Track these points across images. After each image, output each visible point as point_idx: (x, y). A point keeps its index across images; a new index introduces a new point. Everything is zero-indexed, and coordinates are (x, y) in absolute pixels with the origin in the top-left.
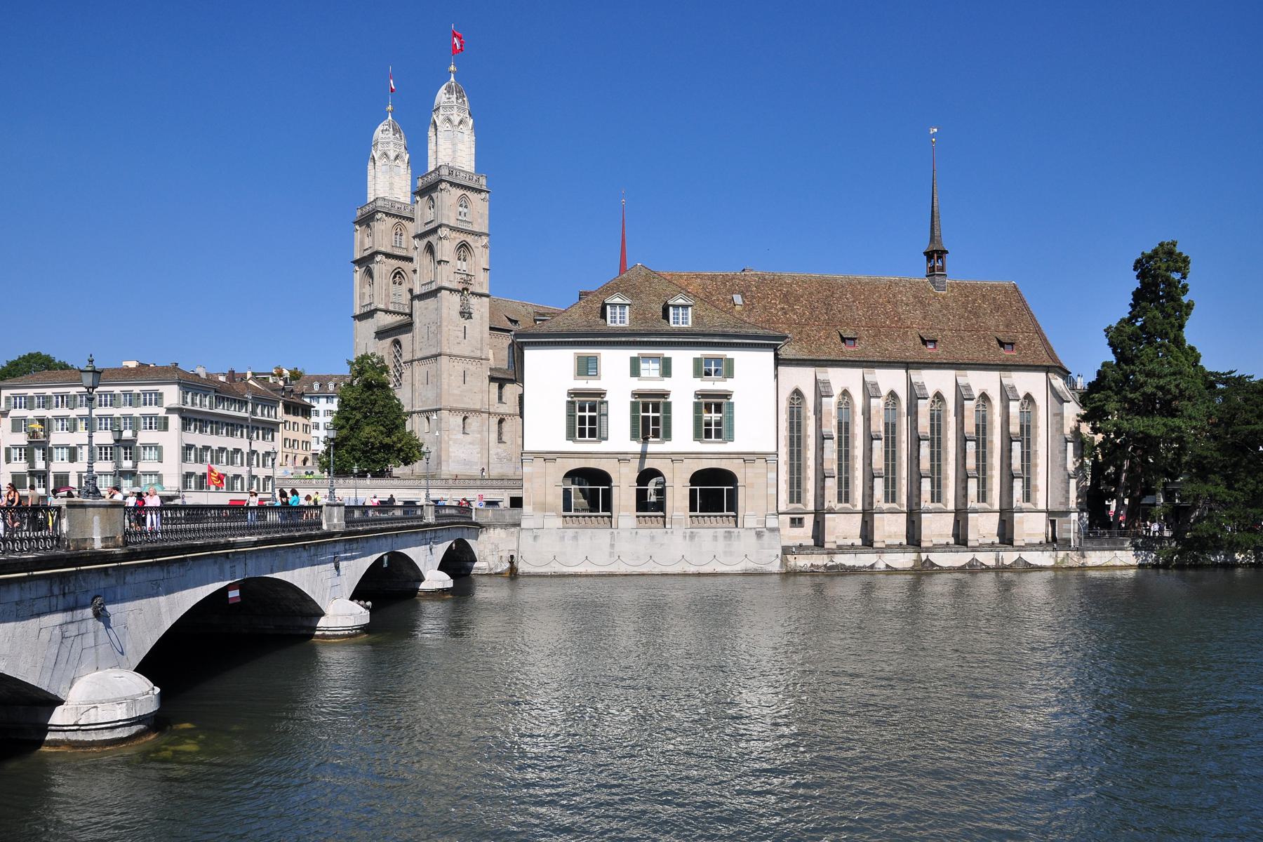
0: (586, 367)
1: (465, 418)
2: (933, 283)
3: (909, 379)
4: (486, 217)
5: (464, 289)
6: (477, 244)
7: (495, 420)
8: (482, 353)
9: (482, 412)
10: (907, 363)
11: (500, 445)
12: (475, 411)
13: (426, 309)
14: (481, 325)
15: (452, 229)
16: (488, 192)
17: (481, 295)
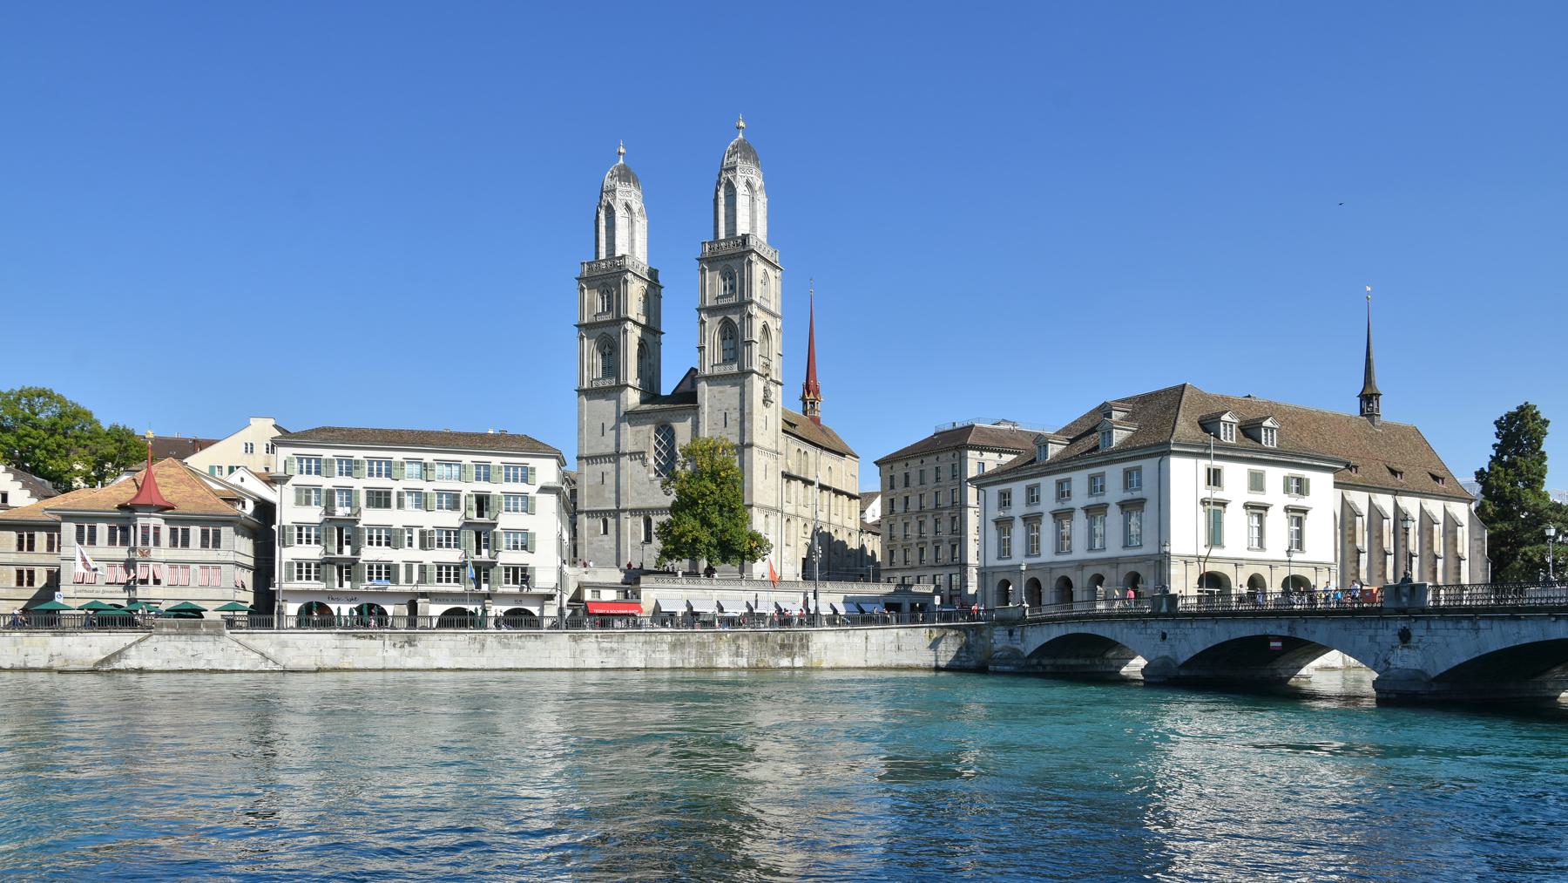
0: (1215, 478)
1: (766, 516)
2: (1372, 422)
3: (1396, 505)
4: (779, 297)
5: (767, 375)
6: (775, 325)
7: (784, 520)
8: (777, 446)
9: (778, 511)
10: (1397, 491)
11: (788, 548)
12: (772, 509)
13: (720, 392)
14: (776, 415)
15: (760, 307)
16: (781, 270)
17: (778, 383)
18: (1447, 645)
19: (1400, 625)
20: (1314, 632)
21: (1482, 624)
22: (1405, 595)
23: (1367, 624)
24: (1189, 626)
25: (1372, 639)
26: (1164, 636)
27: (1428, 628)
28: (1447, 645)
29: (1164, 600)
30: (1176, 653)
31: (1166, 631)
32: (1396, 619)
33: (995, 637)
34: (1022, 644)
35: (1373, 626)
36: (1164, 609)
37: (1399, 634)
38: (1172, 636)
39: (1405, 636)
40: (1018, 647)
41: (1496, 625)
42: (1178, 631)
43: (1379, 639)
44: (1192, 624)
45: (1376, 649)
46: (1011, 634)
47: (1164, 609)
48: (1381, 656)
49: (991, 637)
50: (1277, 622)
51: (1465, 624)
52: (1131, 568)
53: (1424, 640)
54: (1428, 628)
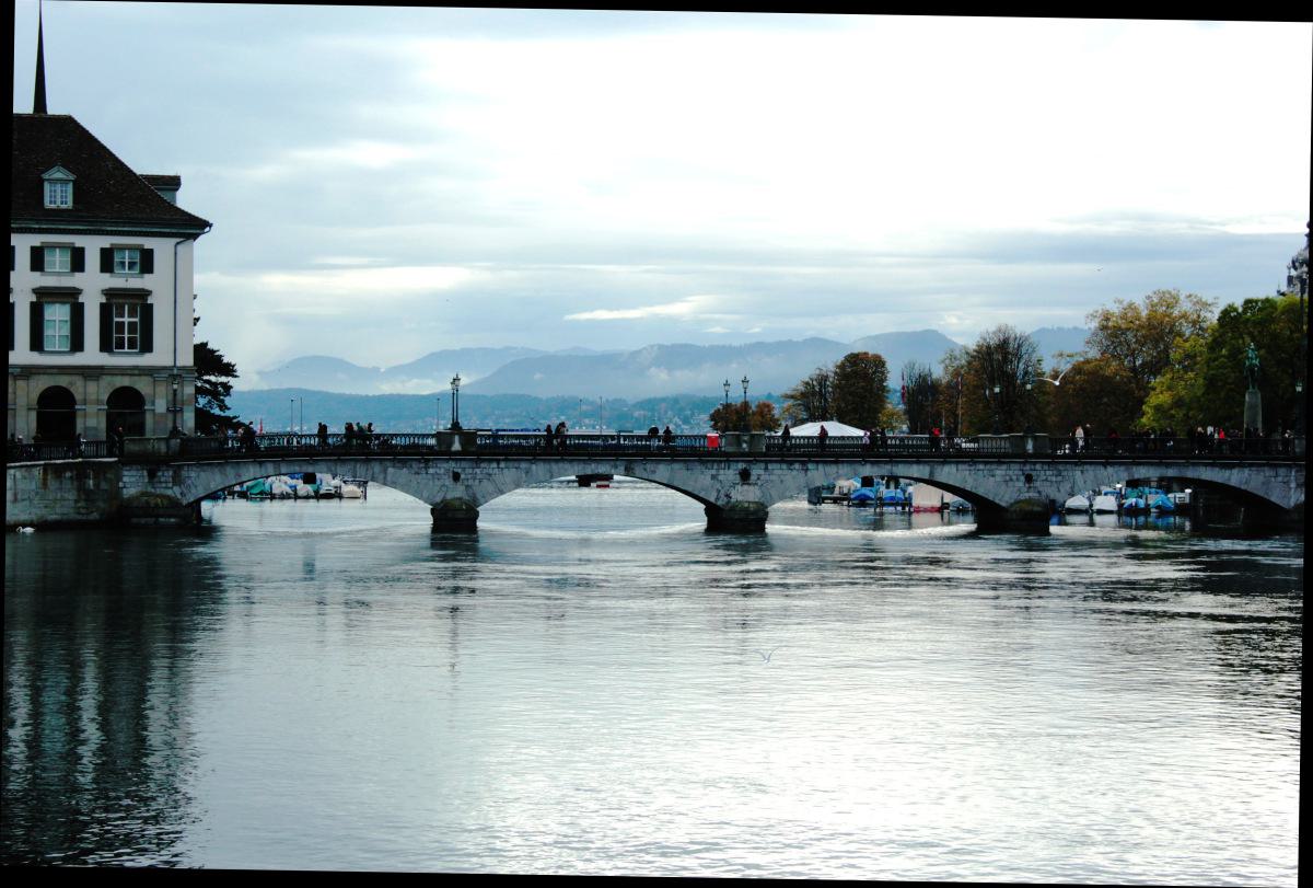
18: (782, 481)
19: (741, 466)
20: (654, 472)
21: (810, 466)
22: (746, 442)
23: (709, 465)
24: (494, 465)
25: (713, 477)
26: (456, 477)
27: (766, 469)
28: (782, 481)
29: (457, 438)
30: (474, 494)
31: (459, 471)
32: (738, 461)
33: (125, 479)
34: (177, 490)
35: (715, 467)
36: (457, 446)
37: (740, 473)
38: (469, 476)
39: (745, 476)
40: (169, 492)
41: (820, 467)
42: (478, 471)
43: (720, 478)
44: (498, 464)
45: (718, 486)
46: (152, 475)
47: (457, 446)
48: (722, 492)
49: (119, 479)
50: (612, 463)
51: (797, 466)
52: (125, 381)
53: (762, 478)
54: (766, 469)
